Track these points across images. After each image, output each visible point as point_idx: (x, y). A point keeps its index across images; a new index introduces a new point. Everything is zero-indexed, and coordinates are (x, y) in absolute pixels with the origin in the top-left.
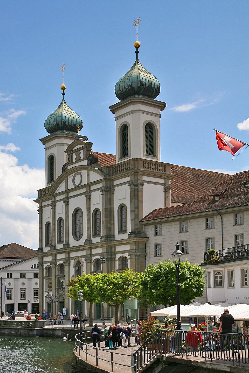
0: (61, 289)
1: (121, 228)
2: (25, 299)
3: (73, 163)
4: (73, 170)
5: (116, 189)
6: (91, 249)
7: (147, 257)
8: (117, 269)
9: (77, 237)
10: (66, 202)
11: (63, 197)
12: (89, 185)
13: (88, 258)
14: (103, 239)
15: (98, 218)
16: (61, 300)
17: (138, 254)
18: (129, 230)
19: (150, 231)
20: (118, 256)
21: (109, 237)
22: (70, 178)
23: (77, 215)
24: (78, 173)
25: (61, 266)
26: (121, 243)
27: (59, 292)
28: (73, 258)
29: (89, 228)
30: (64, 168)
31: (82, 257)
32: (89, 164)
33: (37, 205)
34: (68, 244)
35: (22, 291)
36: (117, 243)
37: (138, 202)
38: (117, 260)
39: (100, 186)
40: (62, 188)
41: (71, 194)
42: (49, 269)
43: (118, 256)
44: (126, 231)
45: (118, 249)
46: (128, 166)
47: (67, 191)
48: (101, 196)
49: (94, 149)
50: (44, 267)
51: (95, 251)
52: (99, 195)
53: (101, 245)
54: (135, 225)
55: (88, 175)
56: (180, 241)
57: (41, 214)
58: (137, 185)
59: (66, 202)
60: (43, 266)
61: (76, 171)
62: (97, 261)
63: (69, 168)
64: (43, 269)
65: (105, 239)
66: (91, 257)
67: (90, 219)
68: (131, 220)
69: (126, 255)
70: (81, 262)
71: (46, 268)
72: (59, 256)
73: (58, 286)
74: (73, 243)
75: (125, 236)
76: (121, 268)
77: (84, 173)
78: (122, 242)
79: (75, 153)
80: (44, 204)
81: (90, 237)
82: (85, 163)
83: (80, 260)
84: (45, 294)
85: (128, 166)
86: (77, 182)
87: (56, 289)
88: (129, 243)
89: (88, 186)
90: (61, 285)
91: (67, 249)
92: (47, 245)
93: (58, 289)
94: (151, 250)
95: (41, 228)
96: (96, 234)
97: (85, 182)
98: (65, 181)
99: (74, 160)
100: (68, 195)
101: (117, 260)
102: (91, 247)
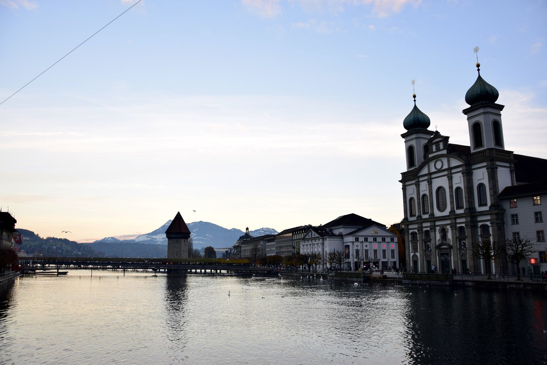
0: (428, 250)
1: (481, 203)
2: (386, 258)
3: (433, 152)
5: (474, 171)
6: (455, 219)
7: (505, 224)
8: (479, 234)
9: (440, 209)
10: (430, 182)
11: (426, 178)
12: (450, 169)
13: (453, 226)
14: (467, 211)
15: (460, 194)
16: (428, 259)
17: (499, 222)
18: (489, 203)
19: (506, 205)
20: (480, 224)
21: (471, 210)
22: (432, 164)
23: (440, 192)
25: (427, 232)
26: (483, 213)
27: (426, 253)
28: (438, 226)
29: (452, 202)
30: (425, 156)
32: (449, 153)
33: (401, 185)
34: (432, 214)
35: (374, 251)
36: (479, 214)
37: (495, 181)
38: (479, 227)
39: (460, 169)
40: (425, 171)
41: (433, 176)
42: (414, 234)
43: (480, 224)
44: (486, 205)
45: (479, 219)
46: (484, 154)
47: (430, 174)
48: (462, 178)
49: (451, 141)
50: (410, 233)
51: (458, 221)
52: (460, 177)
53: (465, 215)
54: (494, 200)
55: (449, 161)
56: (534, 212)
57: (404, 191)
58: (494, 169)
59: (430, 182)
60: (408, 232)
62: (461, 228)
63: (430, 156)
64: (408, 234)
65: (469, 211)
66: (456, 225)
67: (453, 195)
68: (491, 196)
69: (488, 223)
70: (446, 229)
72: (424, 225)
73: (425, 248)
74: (437, 213)
75: (486, 208)
76: (482, 234)
77: (445, 160)
78: (484, 213)
79: (435, 145)
80: (407, 183)
81: (454, 209)
82: (445, 152)
83: (445, 227)
84: (412, 254)
85: (484, 154)
87: (423, 250)
88: (490, 214)
89: (449, 170)
90: (427, 247)
91: (433, 219)
92: (412, 215)
93: (425, 250)
94: (508, 220)
95: (405, 202)
96: (459, 207)
97: (446, 166)
98: (427, 166)
99: (434, 150)
100: (431, 176)
101: (479, 227)
102: (456, 217)
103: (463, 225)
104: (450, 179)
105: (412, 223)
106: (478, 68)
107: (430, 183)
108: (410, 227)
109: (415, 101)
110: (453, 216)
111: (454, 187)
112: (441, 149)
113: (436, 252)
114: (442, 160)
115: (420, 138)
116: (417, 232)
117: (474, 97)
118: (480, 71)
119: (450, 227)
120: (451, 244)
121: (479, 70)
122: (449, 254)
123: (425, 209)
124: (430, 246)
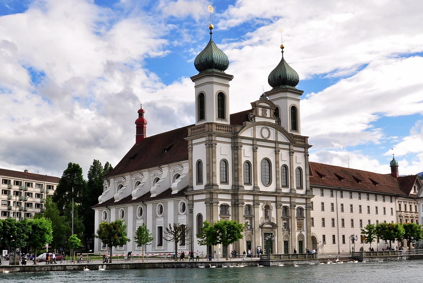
12: (276, 142)
20: (297, 206)
24: (268, 128)
26: (302, 197)
28: (263, 201)
29: (277, 179)
31: (272, 202)
36: (300, 196)
39: (287, 147)
42: (224, 207)
47: (253, 139)
50: (219, 205)
53: (293, 195)
55: (277, 134)
60: (218, 203)
69: (304, 207)
71: (222, 206)
74: (262, 188)
77: (273, 131)
79: (261, 108)
83: (269, 205)
91: (255, 193)
97: (272, 138)
98: (252, 128)
103: (288, 205)
104: (277, 153)
106: (282, 50)
107: (254, 150)
108: (220, 196)
110: (276, 194)
111: (281, 164)
113: (259, 230)
116: (230, 205)
117: (293, 80)
118: (283, 53)
119: (276, 206)
120: (275, 223)
121: (282, 52)
122: (273, 234)
124: (249, 224)
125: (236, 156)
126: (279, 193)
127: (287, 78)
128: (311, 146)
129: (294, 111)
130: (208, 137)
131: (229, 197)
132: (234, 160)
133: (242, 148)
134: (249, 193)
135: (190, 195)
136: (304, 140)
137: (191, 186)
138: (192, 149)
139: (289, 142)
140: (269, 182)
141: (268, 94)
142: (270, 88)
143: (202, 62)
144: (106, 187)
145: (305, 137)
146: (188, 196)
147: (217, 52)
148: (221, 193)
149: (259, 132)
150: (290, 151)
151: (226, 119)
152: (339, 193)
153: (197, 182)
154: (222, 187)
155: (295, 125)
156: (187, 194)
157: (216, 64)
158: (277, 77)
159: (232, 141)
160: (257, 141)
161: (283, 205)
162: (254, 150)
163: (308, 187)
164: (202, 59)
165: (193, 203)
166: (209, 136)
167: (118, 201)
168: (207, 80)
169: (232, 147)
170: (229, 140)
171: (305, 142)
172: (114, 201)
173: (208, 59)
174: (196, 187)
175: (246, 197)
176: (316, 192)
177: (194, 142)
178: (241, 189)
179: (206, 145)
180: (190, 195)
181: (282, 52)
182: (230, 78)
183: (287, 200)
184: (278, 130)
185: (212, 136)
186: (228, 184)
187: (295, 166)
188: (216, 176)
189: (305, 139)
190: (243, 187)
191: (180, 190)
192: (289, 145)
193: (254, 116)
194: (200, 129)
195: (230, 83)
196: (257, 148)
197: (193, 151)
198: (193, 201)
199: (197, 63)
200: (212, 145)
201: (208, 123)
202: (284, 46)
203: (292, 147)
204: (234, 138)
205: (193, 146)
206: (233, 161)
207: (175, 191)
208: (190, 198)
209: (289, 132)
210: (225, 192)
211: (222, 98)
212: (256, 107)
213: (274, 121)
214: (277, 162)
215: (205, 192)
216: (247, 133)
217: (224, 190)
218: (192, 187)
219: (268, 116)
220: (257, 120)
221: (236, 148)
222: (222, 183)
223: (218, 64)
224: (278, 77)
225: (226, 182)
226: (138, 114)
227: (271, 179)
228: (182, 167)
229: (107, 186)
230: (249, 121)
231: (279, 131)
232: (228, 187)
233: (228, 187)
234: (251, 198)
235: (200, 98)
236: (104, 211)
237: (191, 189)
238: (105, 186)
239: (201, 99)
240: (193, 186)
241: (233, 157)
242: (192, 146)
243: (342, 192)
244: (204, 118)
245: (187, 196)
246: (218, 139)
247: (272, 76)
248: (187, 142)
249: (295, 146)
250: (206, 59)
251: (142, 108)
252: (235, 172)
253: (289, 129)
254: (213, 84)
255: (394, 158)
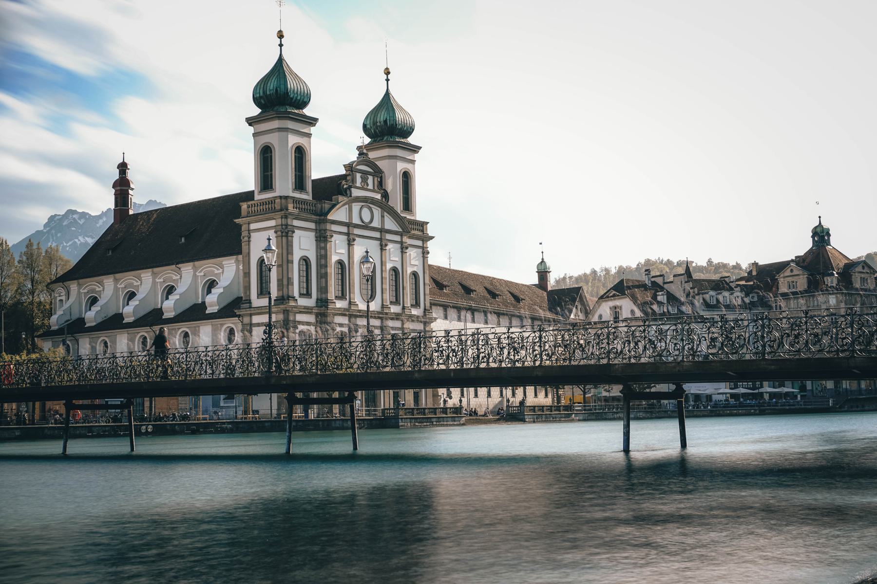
4: (358, 199)
12: (382, 231)
39: (397, 238)
47: (348, 225)
50: (297, 331)
55: (383, 217)
61: (366, 203)
77: (377, 212)
79: (360, 174)
86: (366, 217)
91: (351, 313)
96: (396, 302)
97: (376, 224)
104: (382, 248)
105: (310, 311)
106: (387, 77)
108: (300, 317)
109: (281, 45)
110: (382, 315)
112: (368, 188)
114: (373, 209)
115: (286, 130)
117: (405, 128)
121: (387, 80)
123: (394, 292)
125: (323, 252)
126: (387, 314)
127: (396, 125)
128: (432, 238)
129: (407, 178)
130: (280, 220)
131: (311, 318)
132: (320, 259)
133: (333, 239)
134: (342, 313)
135: (246, 315)
136: (421, 228)
137: (247, 300)
138: (249, 238)
139: (401, 230)
140: (372, 296)
141: (369, 147)
142: (367, 140)
143: (268, 93)
144: (61, 301)
145: (424, 222)
146: (242, 316)
147: (293, 79)
148: (300, 312)
149: (359, 213)
150: (402, 245)
151: (307, 189)
152: (469, 316)
153: (259, 293)
154: (303, 302)
155: (408, 205)
156: (241, 313)
157: (292, 99)
158: (380, 123)
159: (316, 226)
160: (354, 227)
161: (393, 332)
162: (350, 243)
163: (428, 304)
164: (268, 88)
165: (251, 328)
166: (282, 218)
167: (94, 324)
168: (276, 124)
169: (316, 237)
170: (312, 225)
171: (423, 231)
172: (85, 324)
173: (279, 89)
174: (258, 302)
175: (339, 319)
176: (437, 312)
177: (253, 226)
178: (331, 306)
179: (276, 232)
180: (246, 315)
181: (386, 80)
182: (312, 122)
183: (398, 324)
184: (385, 211)
185: (286, 217)
186: (311, 298)
187: (409, 270)
188: (292, 284)
189: (422, 225)
190: (334, 303)
191: (222, 306)
192: (402, 236)
193: (350, 187)
194: (267, 206)
195: (313, 130)
196: (354, 240)
197: (252, 244)
198: (251, 325)
199: (258, 95)
200: (287, 233)
201: (281, 197)
202: (390, 70)
203: (405, 239)
204: (320, 223)
205: (251, 234)
206: (319, 260)
207: (212, 308)
208: (246, 320)
209: (402, 215)
210: (307, 310)
211: (301, 154)
212: (352, 171)
213: (378, 196)
214: (382, 264)
215: (276, 309)
216: (339, 214)
217: (305, 308)
218: (250, 302)
219: (370, 187)
220: (356, 193)
221: (322, 238)
222: (301, 295)
223: (294, 98)
224: (382, 123)
225: (308, 294)
226: (118, 171)
227: (374, 290)
228: (222, 268)
229: (63, 298)
230: (342, 194)
231: (388, 213)
232: (310, 302)
233: (310, 302)
234: (344, 320)
235: (264, 154)
236: (102, 338)
237: (248, 305)
238: (58, 299)
239: (265, 157)
240: (250, 300)
241: (319, 254)
242: (249, 234)
243: (473, 314)
244: (272, 188)
245: (239, 316)
246: (296, 223)
247: (372, 121)
248: (239, 226)
249: (410, 237)
250: (277, 90)
251: (125, 161)
252: (321, 277)
253: (399, 207)
254: (287, 131)
255: (543, 259)
